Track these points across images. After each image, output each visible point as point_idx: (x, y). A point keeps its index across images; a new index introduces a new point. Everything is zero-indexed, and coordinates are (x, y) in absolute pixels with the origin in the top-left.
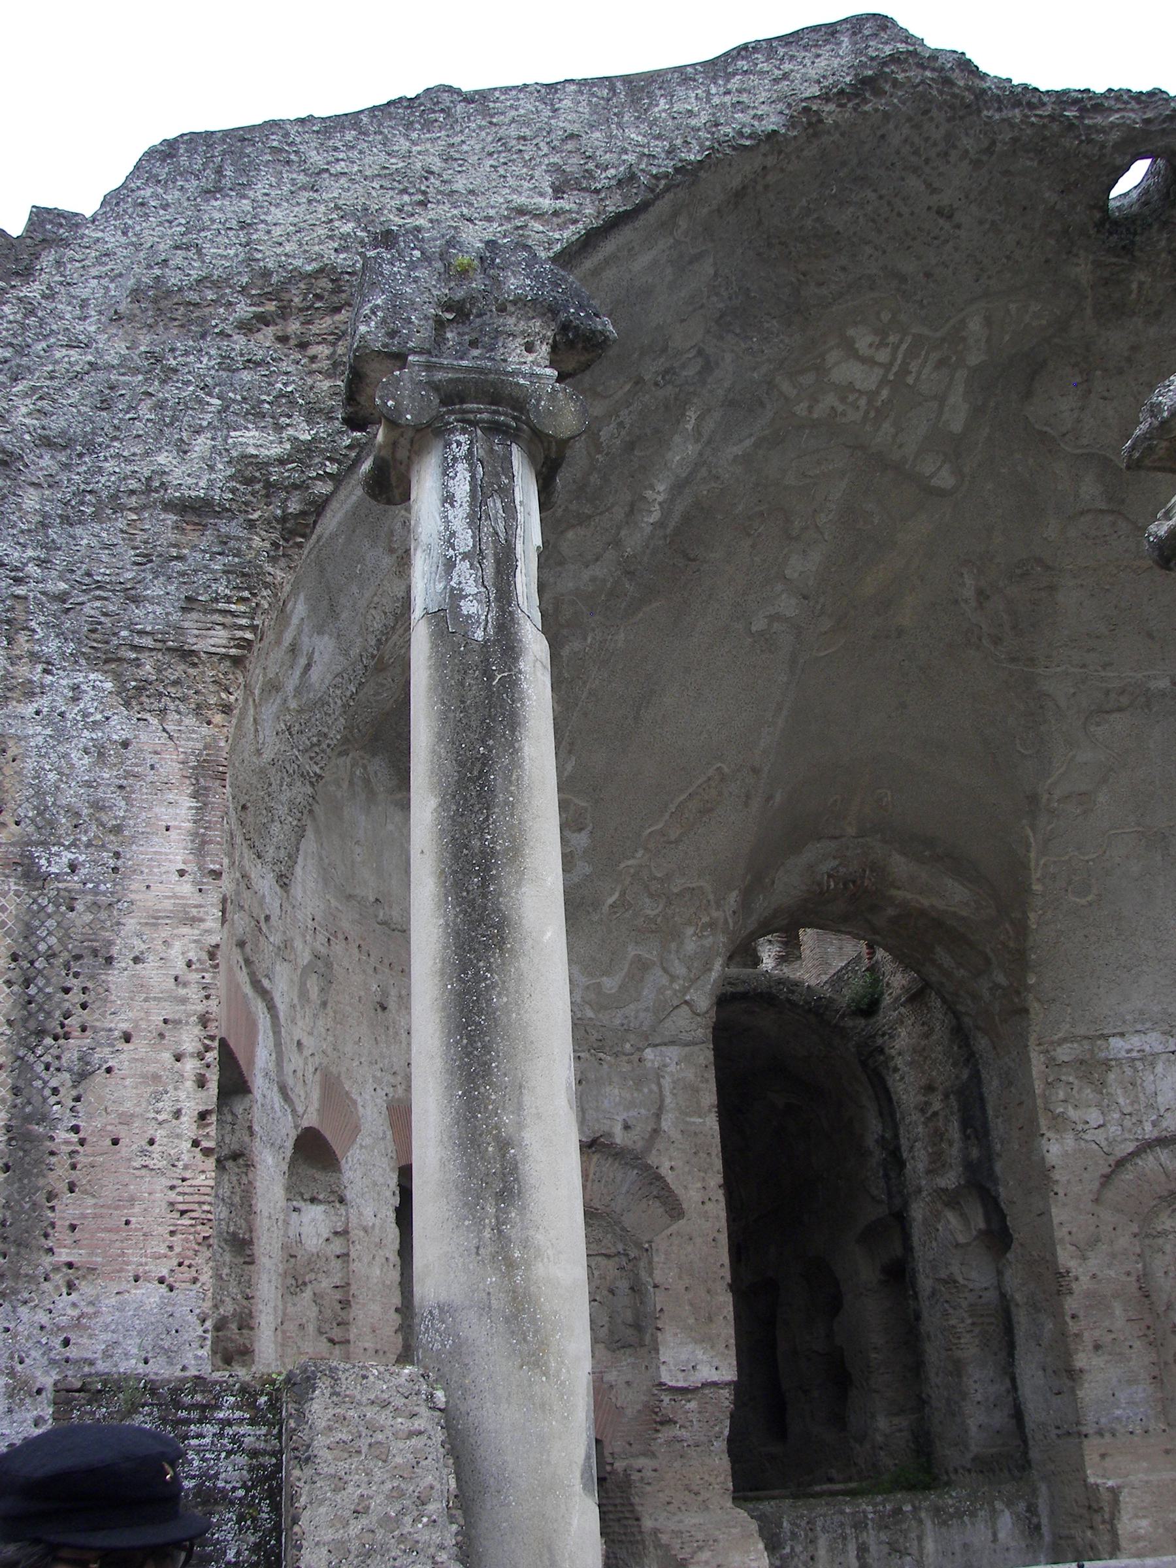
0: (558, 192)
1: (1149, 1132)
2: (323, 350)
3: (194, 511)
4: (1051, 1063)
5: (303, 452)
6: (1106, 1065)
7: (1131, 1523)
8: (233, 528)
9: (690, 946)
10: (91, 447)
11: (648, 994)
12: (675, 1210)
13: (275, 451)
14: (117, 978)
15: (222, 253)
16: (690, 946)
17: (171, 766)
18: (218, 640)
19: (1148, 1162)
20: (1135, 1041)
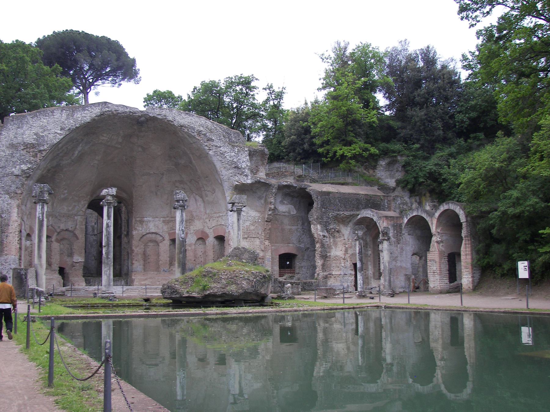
0: (61, 130)
1: (148, 232)
2: (31, 153)
3: (17, 176)
4: (136, 221)
5: (29, 169)
6: (143, 221)
7: (135, 283)
8: (21, 178)
9: (82, 203)
10: (5, 167)
11: (76, 209)
12: (77, 238)
13: (26, 168)
14: (10, 227)
15: (20, 139)
16: (82, 203)
17: (15, 205)
18: (19, 192)
19: (148, 236)
20: (148, 219)
